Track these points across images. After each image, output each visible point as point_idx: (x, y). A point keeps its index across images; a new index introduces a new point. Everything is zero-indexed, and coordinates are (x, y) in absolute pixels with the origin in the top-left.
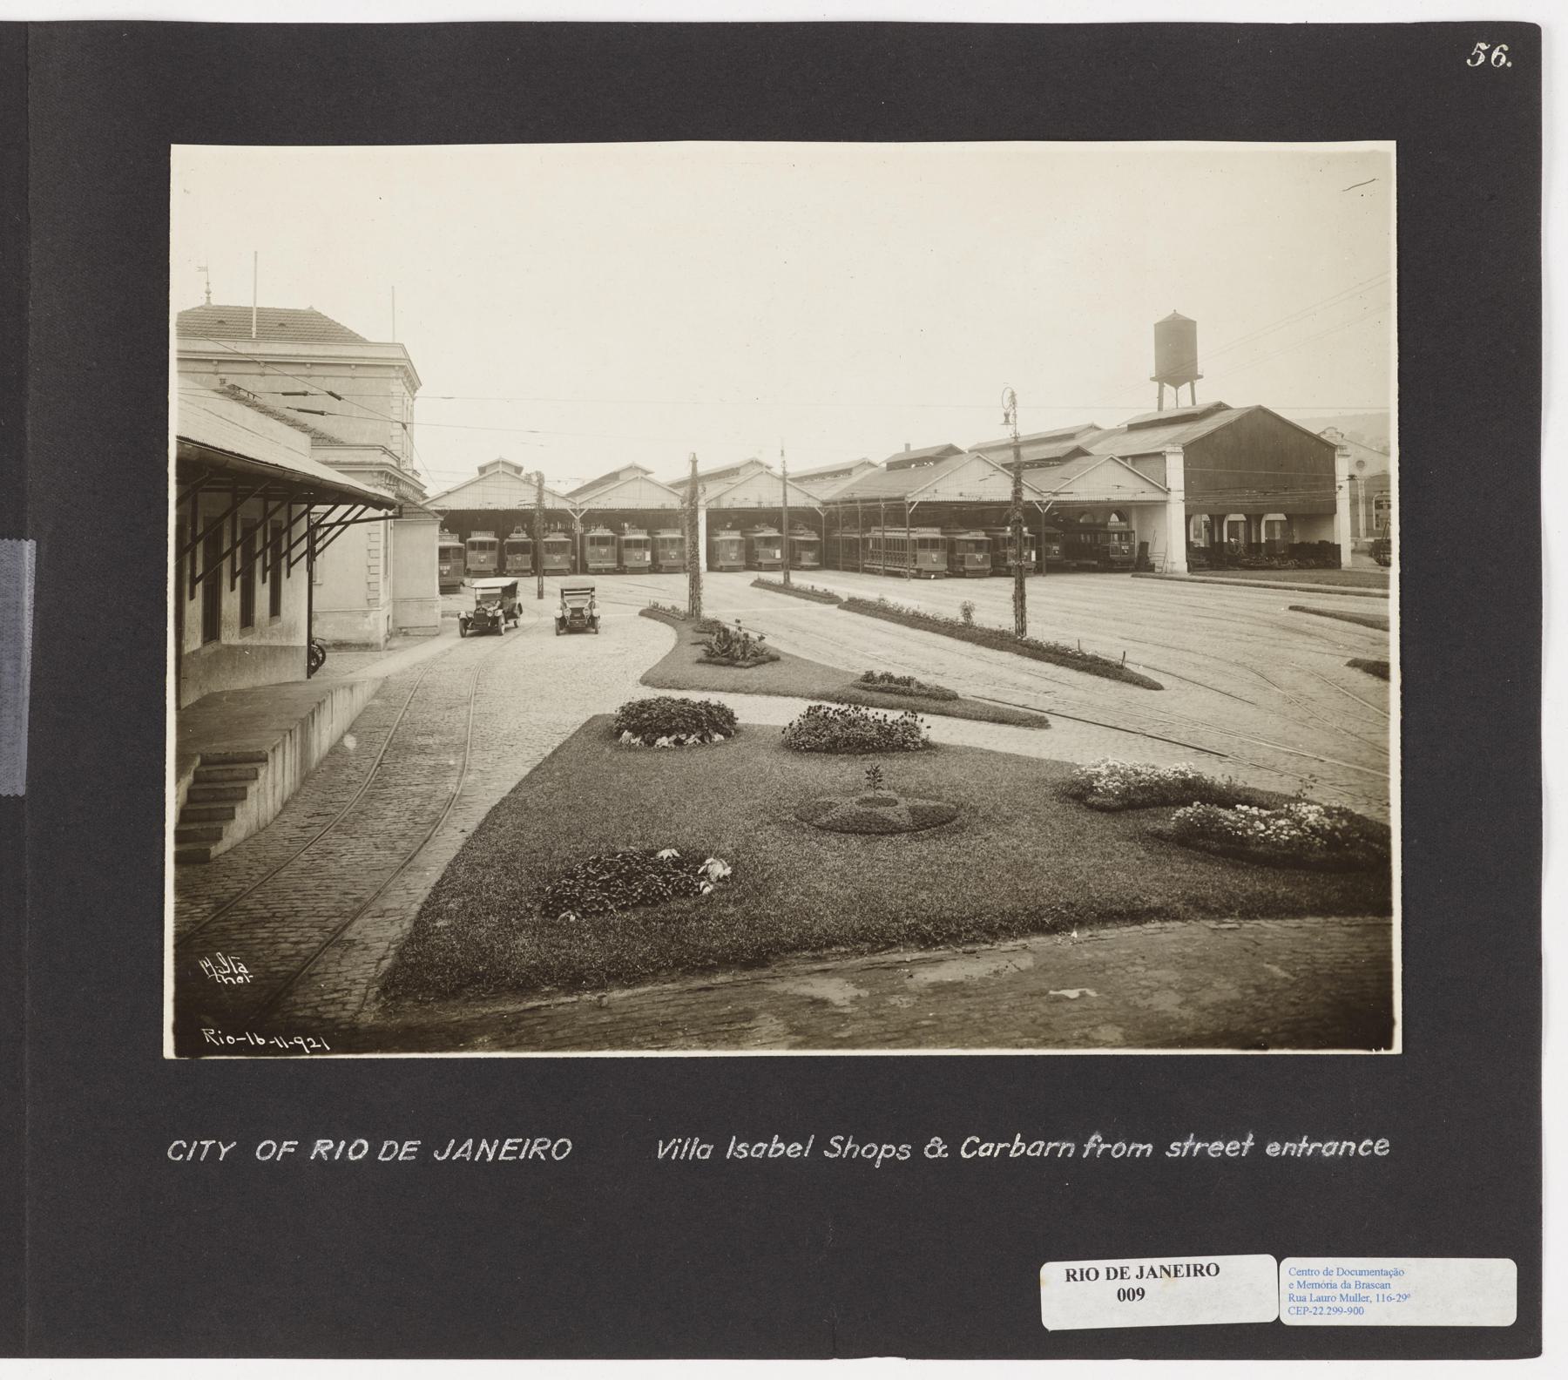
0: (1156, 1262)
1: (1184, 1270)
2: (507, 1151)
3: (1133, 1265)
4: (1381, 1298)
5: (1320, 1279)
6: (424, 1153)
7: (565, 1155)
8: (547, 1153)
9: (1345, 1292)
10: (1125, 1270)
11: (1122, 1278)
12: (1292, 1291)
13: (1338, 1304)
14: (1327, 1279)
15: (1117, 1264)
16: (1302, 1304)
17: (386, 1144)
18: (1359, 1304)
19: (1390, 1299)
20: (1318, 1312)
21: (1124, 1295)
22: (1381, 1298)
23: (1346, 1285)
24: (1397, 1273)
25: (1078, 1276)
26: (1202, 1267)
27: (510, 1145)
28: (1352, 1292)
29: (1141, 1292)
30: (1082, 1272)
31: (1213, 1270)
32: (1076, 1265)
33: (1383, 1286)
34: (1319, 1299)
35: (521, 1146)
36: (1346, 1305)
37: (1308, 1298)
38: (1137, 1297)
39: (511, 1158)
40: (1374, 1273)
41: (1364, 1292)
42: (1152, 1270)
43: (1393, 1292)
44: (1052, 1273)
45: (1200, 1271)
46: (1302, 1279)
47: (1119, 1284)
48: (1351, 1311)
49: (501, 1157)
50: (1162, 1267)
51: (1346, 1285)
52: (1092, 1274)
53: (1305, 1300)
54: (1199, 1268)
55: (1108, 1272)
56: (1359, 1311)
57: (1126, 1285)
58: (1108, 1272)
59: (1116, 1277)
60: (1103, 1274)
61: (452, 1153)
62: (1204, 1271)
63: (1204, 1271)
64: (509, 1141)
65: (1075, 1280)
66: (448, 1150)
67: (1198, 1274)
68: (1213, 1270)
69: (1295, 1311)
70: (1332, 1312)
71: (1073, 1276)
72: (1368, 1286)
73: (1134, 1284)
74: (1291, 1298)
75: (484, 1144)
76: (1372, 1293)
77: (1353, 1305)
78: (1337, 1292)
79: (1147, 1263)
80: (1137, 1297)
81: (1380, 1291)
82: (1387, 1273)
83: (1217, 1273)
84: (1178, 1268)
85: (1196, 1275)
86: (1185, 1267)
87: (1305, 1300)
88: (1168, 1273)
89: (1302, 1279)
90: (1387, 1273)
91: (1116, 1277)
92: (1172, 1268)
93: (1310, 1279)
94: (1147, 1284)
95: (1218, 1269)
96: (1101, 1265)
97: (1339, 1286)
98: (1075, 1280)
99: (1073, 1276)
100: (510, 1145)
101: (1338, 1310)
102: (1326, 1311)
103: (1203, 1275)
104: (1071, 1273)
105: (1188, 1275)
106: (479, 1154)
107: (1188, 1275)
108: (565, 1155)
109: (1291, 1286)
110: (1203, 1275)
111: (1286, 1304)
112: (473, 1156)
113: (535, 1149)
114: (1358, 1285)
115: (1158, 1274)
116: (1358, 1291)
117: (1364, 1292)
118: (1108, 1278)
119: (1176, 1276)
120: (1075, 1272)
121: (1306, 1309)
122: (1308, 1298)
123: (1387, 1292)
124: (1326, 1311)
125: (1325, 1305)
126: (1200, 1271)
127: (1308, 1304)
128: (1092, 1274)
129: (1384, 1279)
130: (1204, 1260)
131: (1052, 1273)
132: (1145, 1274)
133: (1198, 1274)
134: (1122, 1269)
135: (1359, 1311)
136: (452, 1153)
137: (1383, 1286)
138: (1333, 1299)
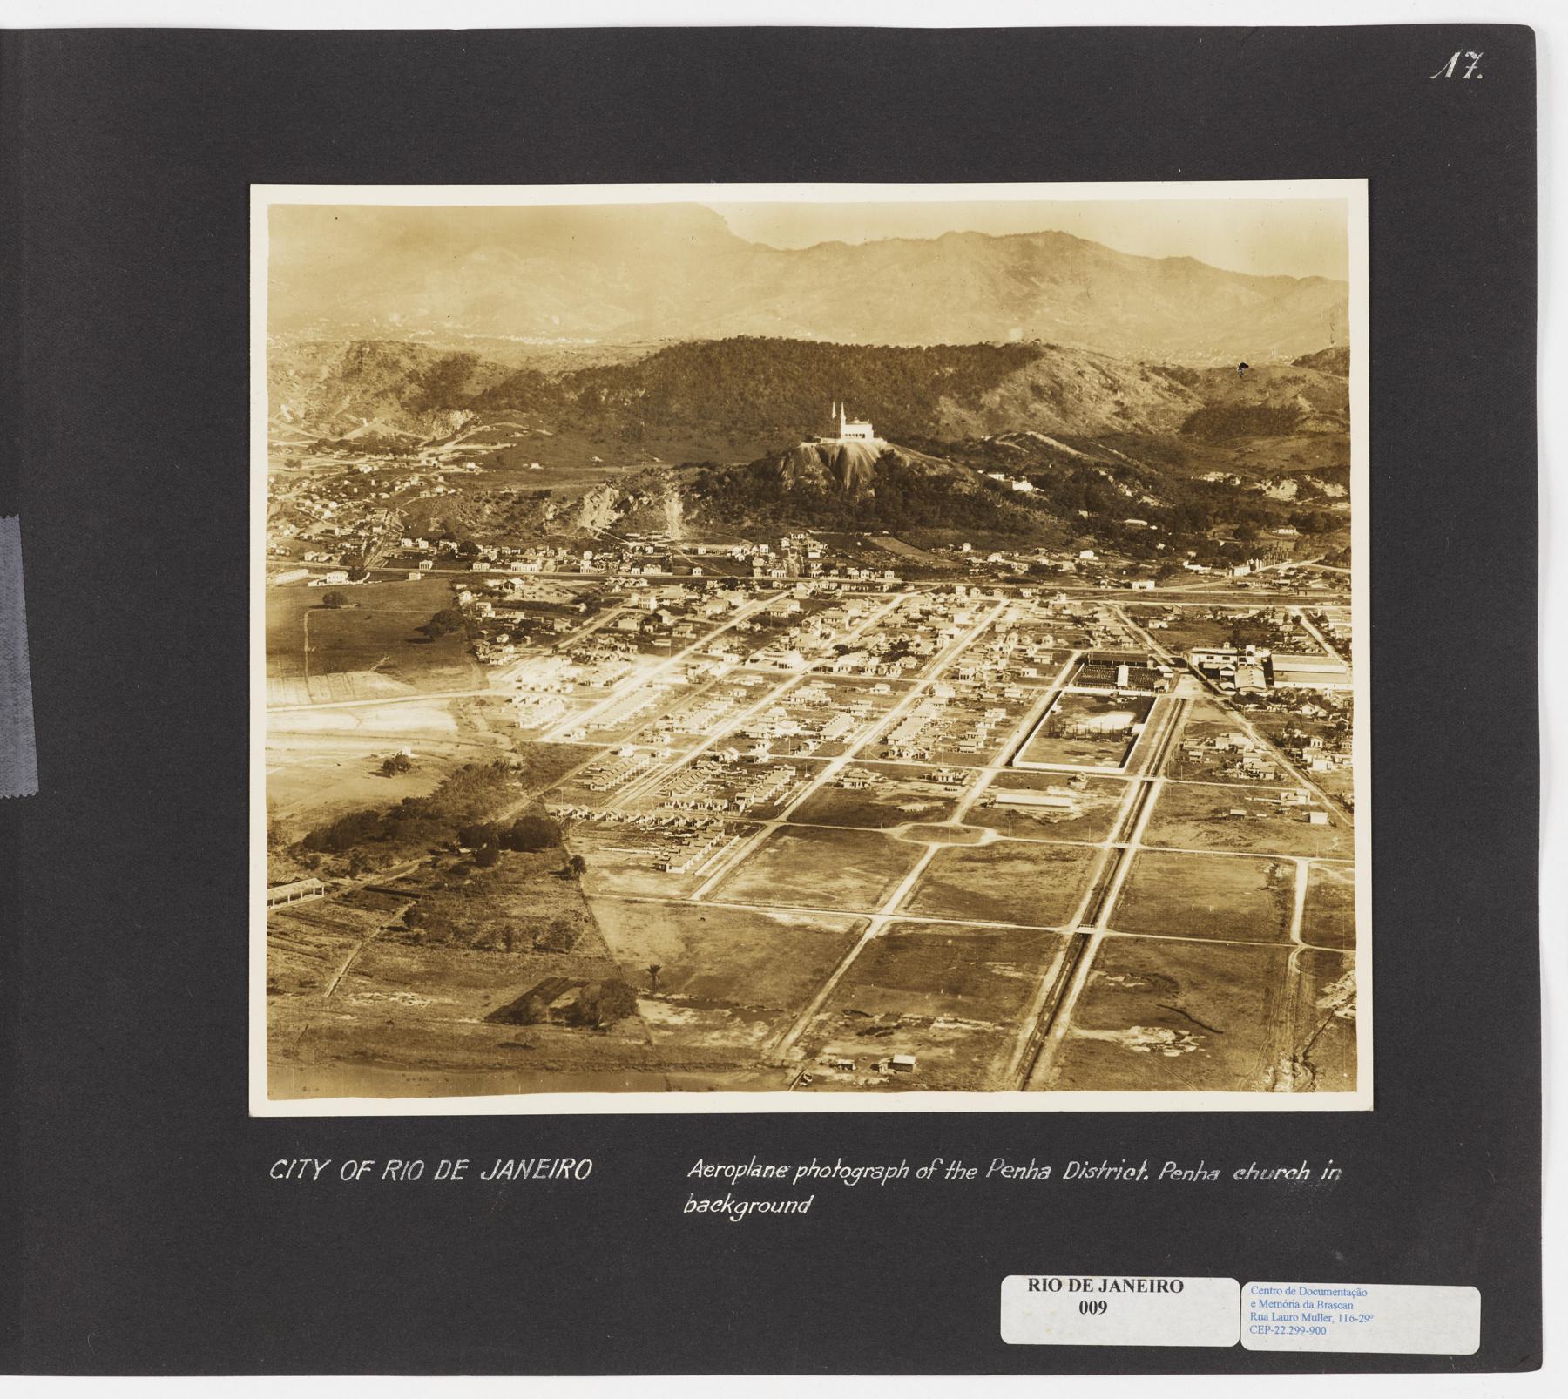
0: (1120, 1280)
1: (1147, 1286)
2: (541, 1170)
3: (1097, 1281)
4: (1343, 1319)
5: (1282, 1298)
6: (470, 1174)
7: (589, 1172)
8: (572, 1171)
9: (1307, 1312)
10: (1088, 1282)
11: (1085, 1290)
12: (1253, 1310)
13: (1300, 1323)
14: (1290, 1298)
15: (1081, 1279)
16: (1264, 1323)
17: (443, 1162)
18: (1321, 1324)
19: (1352, 1319)
20: (1281, 1330)
21: (1086, 1307)
22: (1343, 1319)
23: (1309, 1305)
24: (1360, 1294)
25: (1040, 1286)
26: (1166, 1284)
27: (544, 1163)
28: (1314, 1312)
29: (1103, 1305)
30: (1045, 1284)
31: (1177, 1286)
32: (1040, 1278)
33: (1347, 1307)
34: (1281, 1319)
35: (551, 1164)
36: (1308, 1325)
37: (1270, 1317)
38: (1099, 1310)
39: (543, 1177)
40: (1343, 1293)
41: (1326, 1312)
42: (1115, 1283)
43: (1356, 1313)
44: (1014, 1288)
45: (1164, 1287)
46: (1264, 1298)
47: (1081, 1296)
48: (1313, 1330)
49: (535, 1176)
50: (1126, 1281)
51: (1309, 1305)
52: (1055, 1285)
53: (1267, 1318)
54: (1163, 1283)
55: (1071, 1284)
56: (1320, 1331)
57: (1088, 1297)
58: (1071, 1284)
59: (1078, 1289)
60: (1066, 1286)
61: (498, 1171)
62: (1168, 1287)
63: (1168, 1287)
64: (542, 1160)
65: (1038, 1290)
66: (495, 1172)
67: (1162, 1289)
68: (1177, 1286)
69: (1256, 1330)
70: (1294, 1331)
71: (1035, 1286)
72: (1332, 1306)
73: (1098, 1297)
74: (1253, 1316)
75: (522, 1165)
76: (1334, 1313)
77: (1316, 1324)
78: (1298, 1312)
79: (1111, 1280)
80: (1099, 1310)
81: (1344, 1312)
82: (1350, 1294)
83: (1181, 1290)
84: (1142, 1283)
85: (1159, 1291)
86: (1149, 1282)
87: (1267, 1318)
88: (1132, 1289)
89: (1264, 1298)
90: (1350, 1294)
91: (1078, 1289)
92: (1136, 1283)
93: (1272, 1298)
94: (1110, 1297)
95: (1182, 1286)
96: (1065, 1279)
97: (1301, 1305)
98: (1038, 1290)
99: (1035, 1286)
100: (544, 1163)
101: (1300, 1329)
102: (1288, 1330)
103: (1166, 1291)
104: (1034, 1282)
105: (1152, 1290)
106: (516, 1176)
107: (1152, 1290)
108: (589, 1172)
109: (1253, 1304)
110: (1166, 1291)
111: (1247, 1322)
112: (512, 1176)
113: (565, 1167)
114: (1320, 1304)
115: (1122, 1289)
116: (1320, 1311)
117: (1326, 1312)
118: (1071, 1290)
119: (1139, 1290)
120: (1038, 1282)
121: (1268, 1328)
122: (1270, 1317)
123: (1349, 1312)
124: (1288, 1330)
125: (1287, 1324)
126: (1164, 1287)
127: (1270, 1323)
128: (1055, 1285)
129: (1347, 1300)
130: (1169, 1280)
131: (1014, 1288)
132: (1109, 1286)
133: (1162, 1289)
134: (1085, 1281)
135: (1321, 1331)
136: (497, 1174)
137: (1347, 1307)
138: (1295, 1318)
